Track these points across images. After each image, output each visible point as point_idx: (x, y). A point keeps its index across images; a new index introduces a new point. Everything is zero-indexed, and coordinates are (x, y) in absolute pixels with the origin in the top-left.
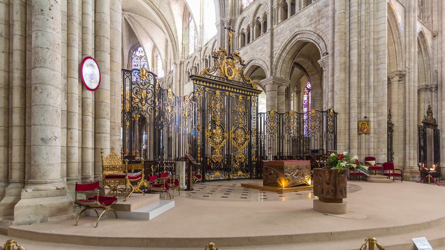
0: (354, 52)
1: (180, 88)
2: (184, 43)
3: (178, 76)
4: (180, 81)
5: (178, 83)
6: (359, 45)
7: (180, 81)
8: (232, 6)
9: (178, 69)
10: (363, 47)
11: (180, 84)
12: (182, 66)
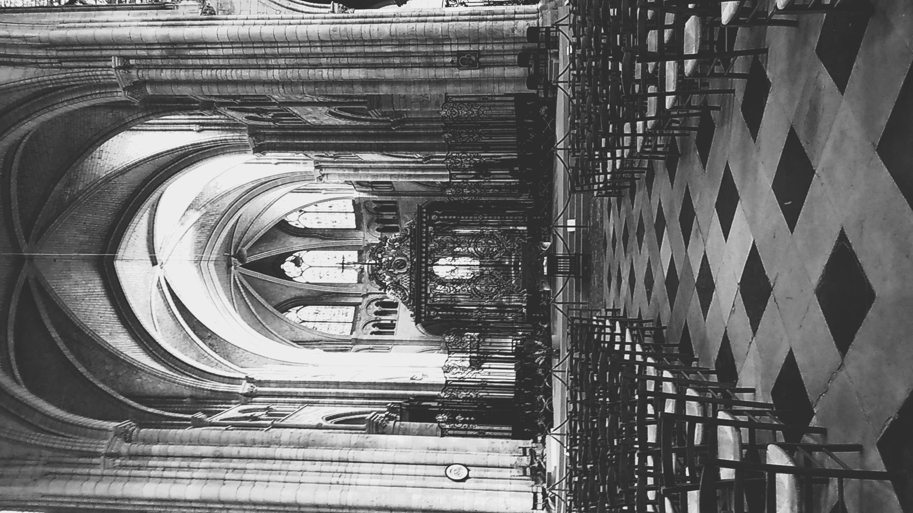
0: (345, 74)
1: (371, 168)
2: (276, 161)
3: (347, 172)
4: (356, 169)
5: (360, 172)
6: (334, 67)
7: (356, 169)
8: (222, 130)
9: (329, 171)
10: (337, 61)
11: (362, 169)
12: (322, 164)
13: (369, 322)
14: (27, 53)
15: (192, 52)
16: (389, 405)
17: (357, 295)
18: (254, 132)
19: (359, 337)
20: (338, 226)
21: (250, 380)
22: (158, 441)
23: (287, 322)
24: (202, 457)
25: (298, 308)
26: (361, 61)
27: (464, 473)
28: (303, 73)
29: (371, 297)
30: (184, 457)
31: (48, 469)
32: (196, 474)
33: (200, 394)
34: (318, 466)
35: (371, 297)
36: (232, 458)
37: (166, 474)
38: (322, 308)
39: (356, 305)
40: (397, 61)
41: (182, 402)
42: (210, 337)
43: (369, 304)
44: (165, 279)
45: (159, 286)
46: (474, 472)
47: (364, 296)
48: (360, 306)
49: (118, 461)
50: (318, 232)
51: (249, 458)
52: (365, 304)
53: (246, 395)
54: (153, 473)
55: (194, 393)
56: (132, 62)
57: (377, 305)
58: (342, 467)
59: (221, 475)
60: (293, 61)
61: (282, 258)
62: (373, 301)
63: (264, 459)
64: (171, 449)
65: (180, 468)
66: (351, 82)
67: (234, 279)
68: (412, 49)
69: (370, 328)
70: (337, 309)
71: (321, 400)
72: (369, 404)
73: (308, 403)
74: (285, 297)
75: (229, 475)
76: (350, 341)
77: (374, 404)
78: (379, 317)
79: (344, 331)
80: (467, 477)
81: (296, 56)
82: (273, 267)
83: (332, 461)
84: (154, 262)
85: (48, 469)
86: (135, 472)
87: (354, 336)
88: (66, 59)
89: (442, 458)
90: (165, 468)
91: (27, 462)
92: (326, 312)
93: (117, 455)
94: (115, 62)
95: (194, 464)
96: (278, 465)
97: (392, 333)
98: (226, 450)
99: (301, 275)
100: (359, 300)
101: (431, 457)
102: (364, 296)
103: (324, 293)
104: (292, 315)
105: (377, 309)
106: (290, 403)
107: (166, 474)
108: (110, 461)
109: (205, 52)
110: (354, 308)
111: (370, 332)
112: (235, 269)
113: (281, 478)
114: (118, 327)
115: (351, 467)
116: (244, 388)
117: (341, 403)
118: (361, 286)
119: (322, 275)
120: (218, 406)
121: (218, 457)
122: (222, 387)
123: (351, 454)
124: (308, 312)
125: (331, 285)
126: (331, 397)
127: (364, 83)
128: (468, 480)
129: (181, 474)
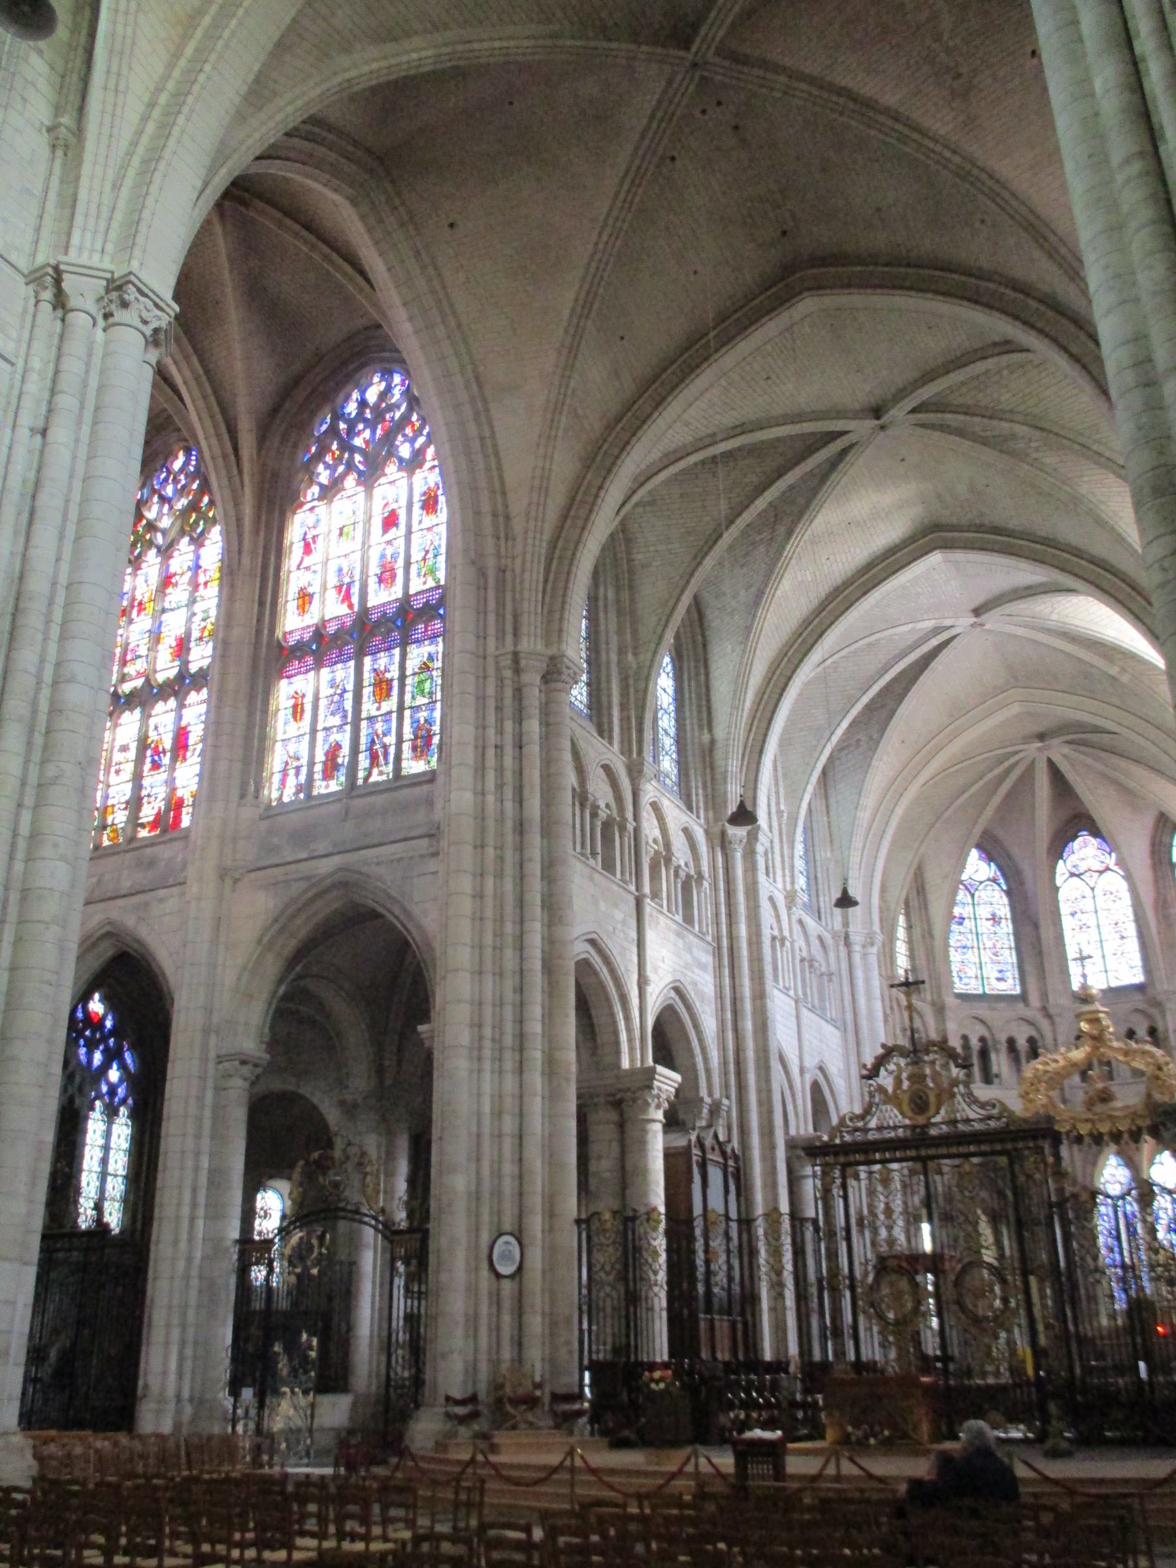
13: (989, 1028)
16: (725, 1101)
17: (1044, 996)
19: (949, 1014)
22: (548, 725)
23: (961, 865)
24: (520, 801)
25: (1002, 881)
27: (506, 1269)
29: (1045, 1024)
32: (490, 799)
33: (719, 755)
34: (510, 996)
35: (1045, 1024)
36: (520, 848)
37: (491, 753)
38: (1007, 927)
41: (701, 727)
42: (871, 738)
43: (1030, 1023)
44: (954, 638)
45: (937, 631)
46: (507, 1286)
47: (1044, 1009)
48: (1021, 1005)
49: (508, 673)
51: (521, 878)
52: (1029, 1013)
55: (720, 744)
57: (1031, 1041)
58: (508, 1040)
59: (491, 839)
62: (1038, 1030)
63: (521, 903)
64: (534, 750)
67: (1017, 753)
69: (975, 1034)
70: (1009, 957)
71: (726, 972)
72: (724, 1063)
73: (719, 947)
74: (1015, 851)
75: (490, 851)
76: (940, 996)
77: (726, 1074)
78: (1003, 1047)
79: (965, 980)
80: (498, 1276)
83: (521, 1022)
84: (977, 612)
86: (491, 704)
87: (950, 1001)
89: (536, 1225)
90: (499, 747)
91: (503, 541)
93: (517, 670)
95: (509, 793)
96: (509, 928)
98: (535, 839)
99: (1072, 875)
100: (1035, 1000)
102: (1044, 1009)
103: (1036, 926)
106: (717, 915)
107: (491, 753)
108: (507, 661)
110: (1017, 991)
111: (967, 1032)
112: (1039, 749)
113: (489, 939)
117: (723, 1009)
118: (1065, 1001)
119: (1078, 916)
120: (700, 791)
121: (521, 828)
123: (536, 1055)
124: (996, 900)
126: (734, 987)
128: (493, 1277)
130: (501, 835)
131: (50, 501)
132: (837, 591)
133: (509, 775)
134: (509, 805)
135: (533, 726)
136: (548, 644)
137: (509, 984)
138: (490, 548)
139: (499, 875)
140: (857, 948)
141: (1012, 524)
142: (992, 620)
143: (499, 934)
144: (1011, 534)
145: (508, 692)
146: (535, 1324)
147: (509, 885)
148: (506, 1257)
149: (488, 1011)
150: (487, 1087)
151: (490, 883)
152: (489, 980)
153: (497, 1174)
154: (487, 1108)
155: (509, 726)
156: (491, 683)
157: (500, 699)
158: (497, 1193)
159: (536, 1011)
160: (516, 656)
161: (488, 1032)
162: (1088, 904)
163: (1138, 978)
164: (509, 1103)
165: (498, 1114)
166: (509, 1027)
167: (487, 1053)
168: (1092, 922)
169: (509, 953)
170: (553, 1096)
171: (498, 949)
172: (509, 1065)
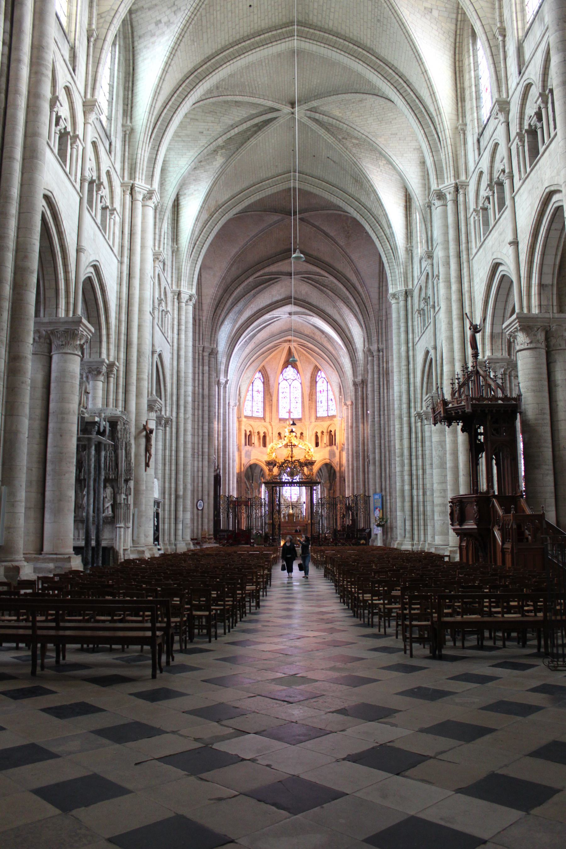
14: (384, 307)
15: (385, 382)
18: (364, 382)
20: (319, 404)
21: (227, 382)
24: (203, 389)
26: (383, 458)
27: (200, 508)
28: (376, 432)
30: (203, 381)
31: (197, 321)
32: (197, 388)
34: (200, 442)
36: (203, 403)
37: (197, 375)
38: (261, 394)
39: (264, 418)
40: (383, 475)
43: (266, 427)
46: (200, 512)
49: (201, 352)
50: (314, 391)
53: (219, 381)
54: (197, 369)
56: (381, 353)
57: (264, 433)
58: (200, 453)
59: (196, 400)
60: (382, 427)
61: (295, 366)
63: (203, 418)
64: (206, 375)
65: (199, 380)
66: (374, 453)
68: (388, 482)
69: (249, 429)
70: (261, 405)
74: (269, 370)
75: (196, 403)
81: (384, 429)
82: (290, 362)
84: (290, 314)
85: (197, 321)
86: (197, 360)
87: (244, 420)
88: (382, 323)
89: (206, 498)
92: (259, 397)
93: (203, 351)
94: (381, 346)
96: (201, 424)
97: (246, 445)
98: (206, 400)
101: (206, 493)
103: (271, 396)
104: (258, 375)
105: (262, 435)
108: (201, 349)
109: (385, 388)
113: (196, 427)
114: (255, 309)
115: (200, 457)
116: (222, 380)
122: (223, 367)
124: (259, 385)
125: (278, 400)
127: (374, 459)
129: (197, 382)
130: (199, 398)
131: (182, 353)
132: (260, 310)
133: (201, 382)
134: (201, 390)
135: (206, 368)
136: (210, 344)
137: (200, 439)
138: (197, 313)
139: (198, 410)
140: (231, 407)
141: (315, 303)
142: (294, 317)
143: (198, 426)
144: (313, 305)
145: (201, 357)
146: (206, 520)
147: (200, 412)
148: (200, 505)
149: (196, 445)
150: (196, 464)
151: (196, 411)
152: (196, 437)
153: (198, 486)
154: (196, 470)
155: (201, 367)
156: (197, 354)
157: (199, 359)
158: (198, 490)
159: (206, 446)
160: (204, 347)
161: (196, 451)
162: (287, 390)
163: (300, 417)
164: (200, 469)
165: (198, 471)
166: (200, 450)
167: (196, 456)
168: (288, 396)
169: (200, 431)
170: (209, 467)
171: (198, 429)
172: (200, 459)
